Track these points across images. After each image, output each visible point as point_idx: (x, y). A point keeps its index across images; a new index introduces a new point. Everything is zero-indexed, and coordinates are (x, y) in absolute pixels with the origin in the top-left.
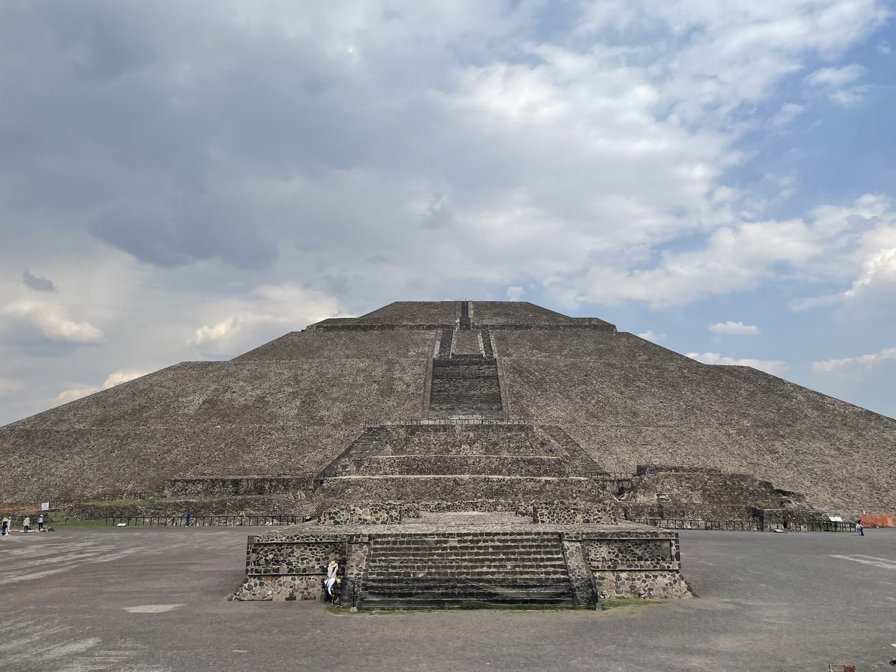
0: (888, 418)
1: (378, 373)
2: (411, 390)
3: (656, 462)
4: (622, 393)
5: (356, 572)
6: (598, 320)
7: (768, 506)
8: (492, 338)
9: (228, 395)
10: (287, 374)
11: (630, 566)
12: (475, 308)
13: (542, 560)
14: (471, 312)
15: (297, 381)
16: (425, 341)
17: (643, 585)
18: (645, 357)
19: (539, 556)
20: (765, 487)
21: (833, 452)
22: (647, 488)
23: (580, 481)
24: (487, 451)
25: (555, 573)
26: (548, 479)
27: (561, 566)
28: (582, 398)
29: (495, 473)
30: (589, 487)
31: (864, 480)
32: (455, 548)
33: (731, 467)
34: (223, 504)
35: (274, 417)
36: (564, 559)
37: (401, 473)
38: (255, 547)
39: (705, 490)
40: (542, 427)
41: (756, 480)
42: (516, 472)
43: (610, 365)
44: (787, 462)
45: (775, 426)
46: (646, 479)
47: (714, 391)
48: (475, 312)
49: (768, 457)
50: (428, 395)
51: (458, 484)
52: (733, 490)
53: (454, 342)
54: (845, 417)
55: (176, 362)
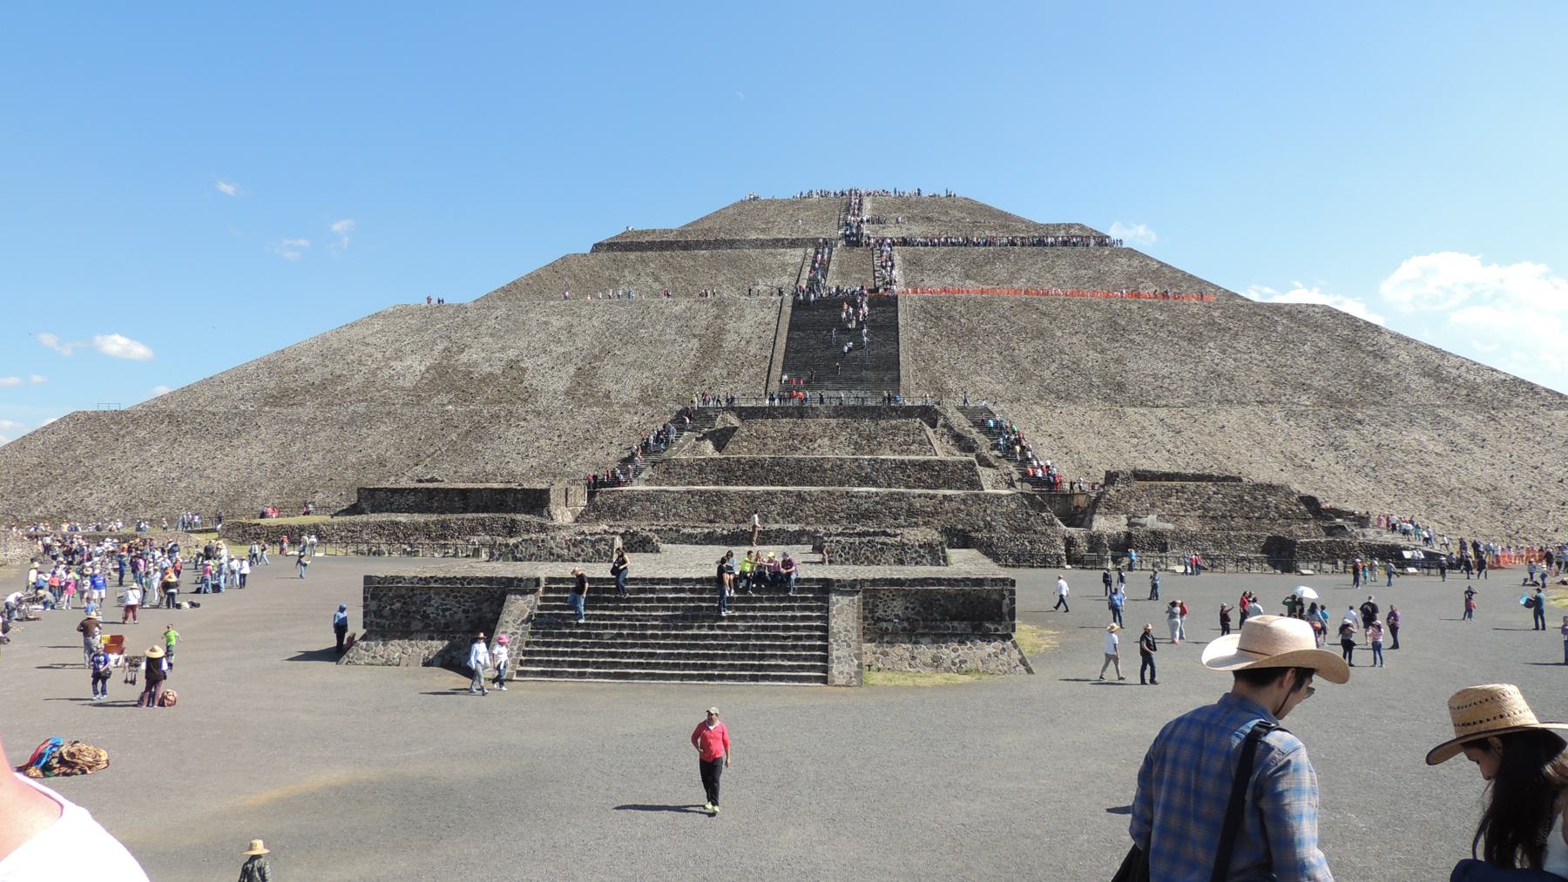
0: (1548, 391)
2: (753, 349)
3: (1145, 465)
4: (1102, 352)
5: (510, 631)
6: (1082, 227)
7: (1307, 533)
9: (464, 358)
10: (557, 322)
11: (939, 628)
12: (873, 209)
13: (794, 618)
16: (783, 267)
17: (953, 655)
19: (790, 614)
20: (1306, 504)
21: (1439, 449)
22: (1113, 508)
23: (999, 497)
24: (858, 448)
25: (809, 637)
26: (948, 492)
27: (817, 628)
28: (1035, 361)
29: (866, 484)
30: (1013, 506)
31: (1486, 493)
32: (665, 600)
33: (1263, 470)
34: (444, 525)
36: (826, 619)
37: (716, 483)
38: (375, 590)
39: (1207, 510)
40: (961, 409)
41: (1292, 493)
42: (898, 482)
44: (1360, 462)
46: (1112, 492)
49: (1331, 456)
50: (779, 357)
51: (804, 500)
52: (1252, 509)
54: (1474, 388)
55: (387, 305)
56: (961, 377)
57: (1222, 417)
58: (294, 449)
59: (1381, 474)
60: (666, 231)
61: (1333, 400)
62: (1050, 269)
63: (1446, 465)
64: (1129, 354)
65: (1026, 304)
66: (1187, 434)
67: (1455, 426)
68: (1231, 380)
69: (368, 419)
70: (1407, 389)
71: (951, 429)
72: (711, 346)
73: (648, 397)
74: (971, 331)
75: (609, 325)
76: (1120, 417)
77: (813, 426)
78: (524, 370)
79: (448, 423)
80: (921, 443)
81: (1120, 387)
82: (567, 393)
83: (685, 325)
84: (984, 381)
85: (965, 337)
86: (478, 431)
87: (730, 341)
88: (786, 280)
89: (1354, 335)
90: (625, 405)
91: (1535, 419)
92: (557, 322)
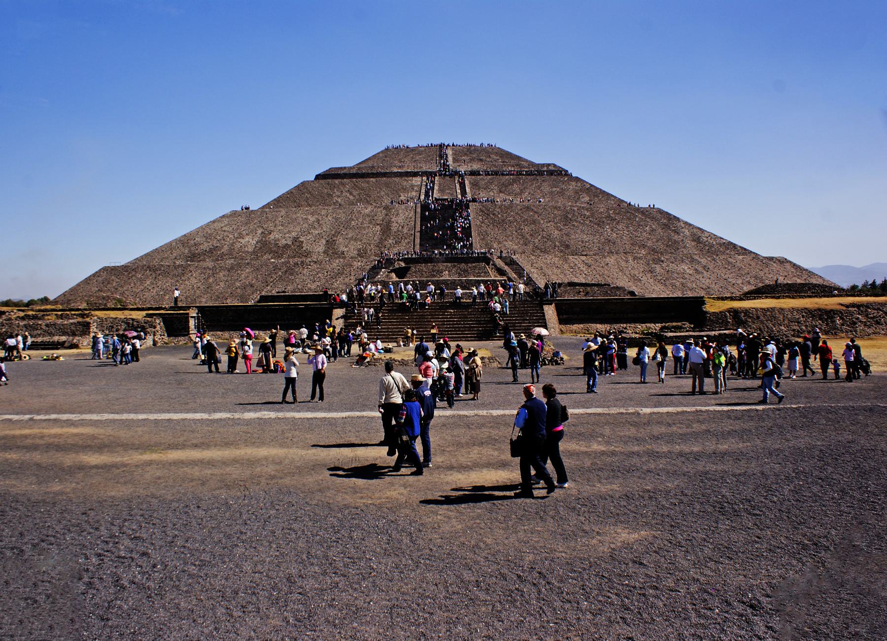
1: (380, 217)
6: (555, 165)
8: (467, 182)
9: (272, 237)
10: (312, 219)
12: (453, 154)
14: (450, 159)
15: (320, 225)
16: (412, 187)
18: (587, 199)
21: (691, 272)
24: (460, 275)
28: (531, 235)
35: (308, 254)
40: (500, 257)
43: (555, 208)
45: (662, 254)
47: (627, 227)
48: (454, 159)
49: (649, 275)
53: (436, 187)
55: (227, 211)
56: (499, 243)
57: (608, 259)
58: (211, 280)
59: (667, 283)
60: (351, 168)
61: (654, 250)
62: (539, 187)
63: (692, 279)
64: (572, 232)
65: (528, 207)
66: (593, 267)
67: (699, 262)
68: (614, 243)
69: (239, 265)
70: (684, 247)
71: (496, 266)
72: (386, 229)
73: (361, 254)
74: (503, 221)
75: (336, 219)
76: (566, 260)
77: (441, 266)
78: (302, 242)
79: (276, 267)
80: (485, 273)
81: (567, 247)
82: (324, 252)
83: (372, 218)
84: (509, 244)
85: (501, 224)
86: (290, 271)
87: (394, 227)
88: (414, 194)
89: (668, 221)
90: (352, 258)
91: (730, 260)
92: (312, 219)
